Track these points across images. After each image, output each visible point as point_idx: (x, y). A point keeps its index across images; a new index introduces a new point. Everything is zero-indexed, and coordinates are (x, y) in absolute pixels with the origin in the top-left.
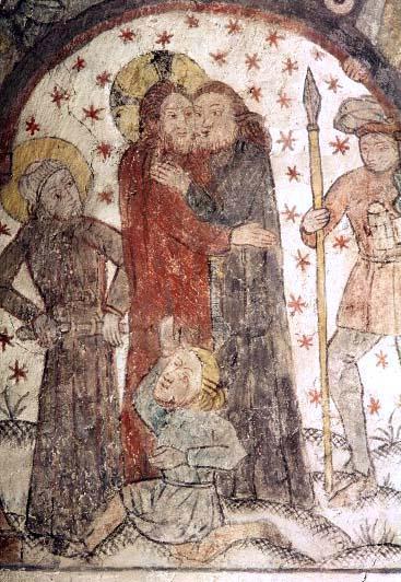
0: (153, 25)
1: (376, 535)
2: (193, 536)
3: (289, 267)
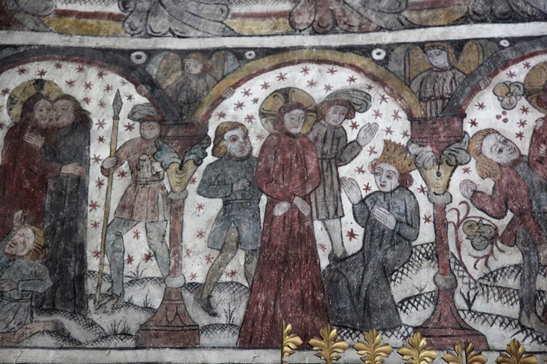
0: (37, 67)
1: (119, 328)
2: (13, 328)
3: (92, 186)
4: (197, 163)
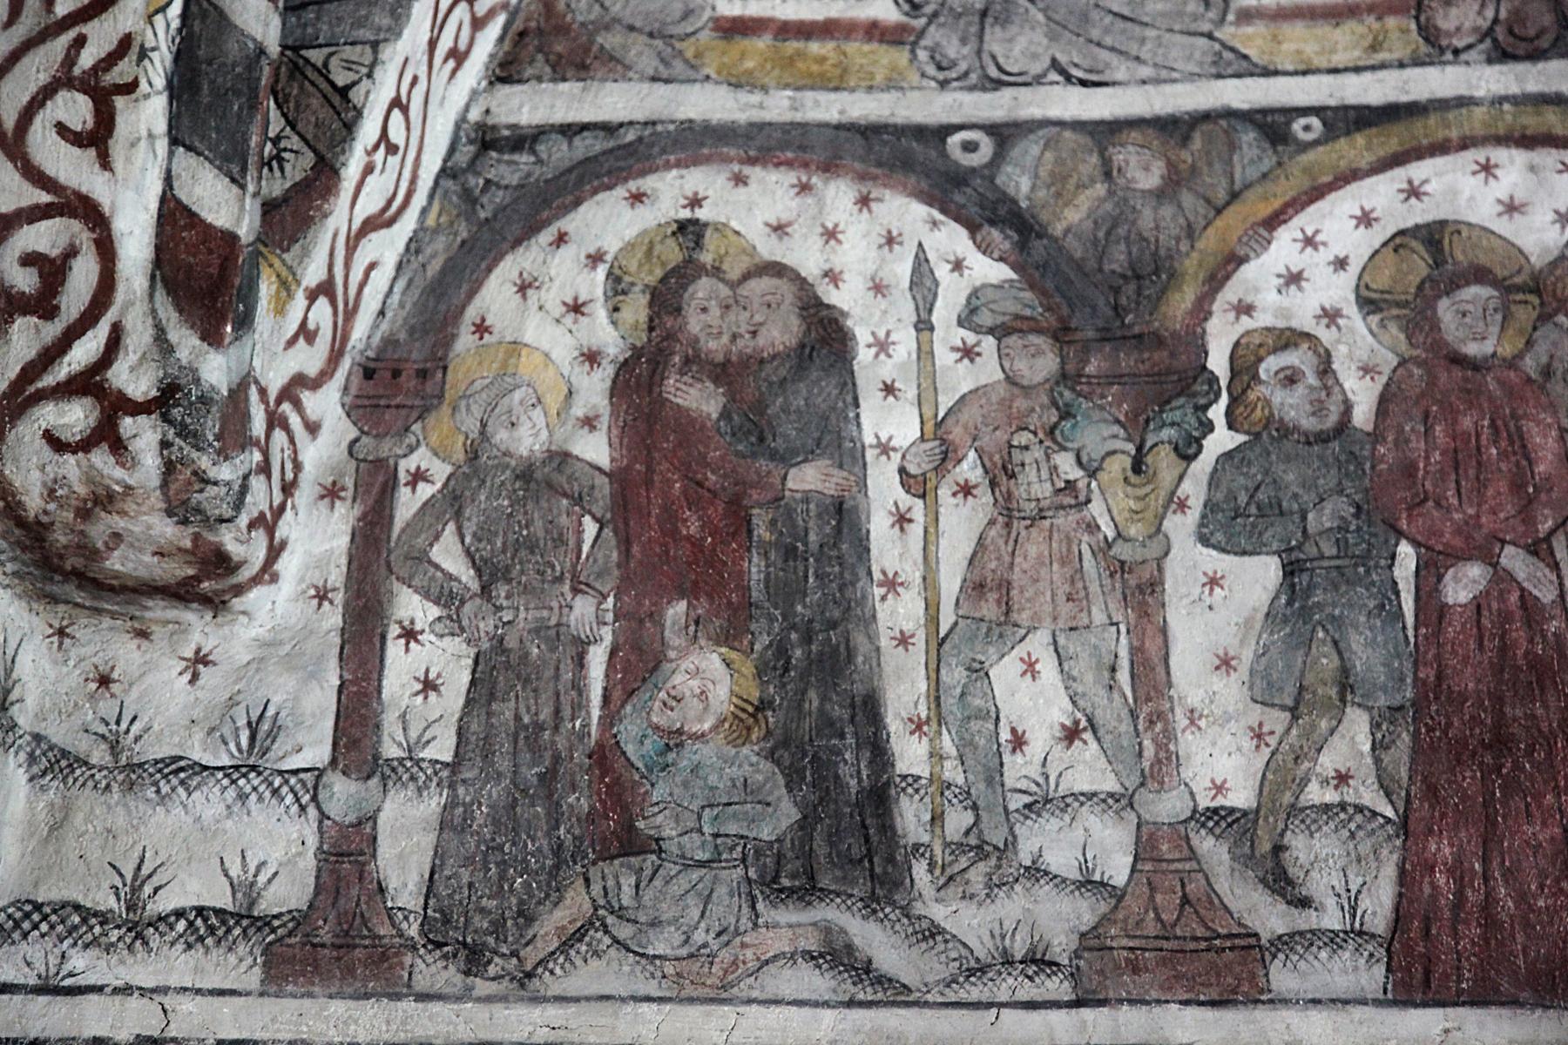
0: (678, 182)
1: (1017, 945)
2: (705, 945)
3: (879, 526)
4: (1187, 451)
